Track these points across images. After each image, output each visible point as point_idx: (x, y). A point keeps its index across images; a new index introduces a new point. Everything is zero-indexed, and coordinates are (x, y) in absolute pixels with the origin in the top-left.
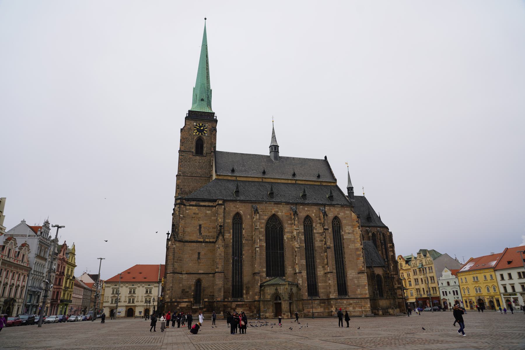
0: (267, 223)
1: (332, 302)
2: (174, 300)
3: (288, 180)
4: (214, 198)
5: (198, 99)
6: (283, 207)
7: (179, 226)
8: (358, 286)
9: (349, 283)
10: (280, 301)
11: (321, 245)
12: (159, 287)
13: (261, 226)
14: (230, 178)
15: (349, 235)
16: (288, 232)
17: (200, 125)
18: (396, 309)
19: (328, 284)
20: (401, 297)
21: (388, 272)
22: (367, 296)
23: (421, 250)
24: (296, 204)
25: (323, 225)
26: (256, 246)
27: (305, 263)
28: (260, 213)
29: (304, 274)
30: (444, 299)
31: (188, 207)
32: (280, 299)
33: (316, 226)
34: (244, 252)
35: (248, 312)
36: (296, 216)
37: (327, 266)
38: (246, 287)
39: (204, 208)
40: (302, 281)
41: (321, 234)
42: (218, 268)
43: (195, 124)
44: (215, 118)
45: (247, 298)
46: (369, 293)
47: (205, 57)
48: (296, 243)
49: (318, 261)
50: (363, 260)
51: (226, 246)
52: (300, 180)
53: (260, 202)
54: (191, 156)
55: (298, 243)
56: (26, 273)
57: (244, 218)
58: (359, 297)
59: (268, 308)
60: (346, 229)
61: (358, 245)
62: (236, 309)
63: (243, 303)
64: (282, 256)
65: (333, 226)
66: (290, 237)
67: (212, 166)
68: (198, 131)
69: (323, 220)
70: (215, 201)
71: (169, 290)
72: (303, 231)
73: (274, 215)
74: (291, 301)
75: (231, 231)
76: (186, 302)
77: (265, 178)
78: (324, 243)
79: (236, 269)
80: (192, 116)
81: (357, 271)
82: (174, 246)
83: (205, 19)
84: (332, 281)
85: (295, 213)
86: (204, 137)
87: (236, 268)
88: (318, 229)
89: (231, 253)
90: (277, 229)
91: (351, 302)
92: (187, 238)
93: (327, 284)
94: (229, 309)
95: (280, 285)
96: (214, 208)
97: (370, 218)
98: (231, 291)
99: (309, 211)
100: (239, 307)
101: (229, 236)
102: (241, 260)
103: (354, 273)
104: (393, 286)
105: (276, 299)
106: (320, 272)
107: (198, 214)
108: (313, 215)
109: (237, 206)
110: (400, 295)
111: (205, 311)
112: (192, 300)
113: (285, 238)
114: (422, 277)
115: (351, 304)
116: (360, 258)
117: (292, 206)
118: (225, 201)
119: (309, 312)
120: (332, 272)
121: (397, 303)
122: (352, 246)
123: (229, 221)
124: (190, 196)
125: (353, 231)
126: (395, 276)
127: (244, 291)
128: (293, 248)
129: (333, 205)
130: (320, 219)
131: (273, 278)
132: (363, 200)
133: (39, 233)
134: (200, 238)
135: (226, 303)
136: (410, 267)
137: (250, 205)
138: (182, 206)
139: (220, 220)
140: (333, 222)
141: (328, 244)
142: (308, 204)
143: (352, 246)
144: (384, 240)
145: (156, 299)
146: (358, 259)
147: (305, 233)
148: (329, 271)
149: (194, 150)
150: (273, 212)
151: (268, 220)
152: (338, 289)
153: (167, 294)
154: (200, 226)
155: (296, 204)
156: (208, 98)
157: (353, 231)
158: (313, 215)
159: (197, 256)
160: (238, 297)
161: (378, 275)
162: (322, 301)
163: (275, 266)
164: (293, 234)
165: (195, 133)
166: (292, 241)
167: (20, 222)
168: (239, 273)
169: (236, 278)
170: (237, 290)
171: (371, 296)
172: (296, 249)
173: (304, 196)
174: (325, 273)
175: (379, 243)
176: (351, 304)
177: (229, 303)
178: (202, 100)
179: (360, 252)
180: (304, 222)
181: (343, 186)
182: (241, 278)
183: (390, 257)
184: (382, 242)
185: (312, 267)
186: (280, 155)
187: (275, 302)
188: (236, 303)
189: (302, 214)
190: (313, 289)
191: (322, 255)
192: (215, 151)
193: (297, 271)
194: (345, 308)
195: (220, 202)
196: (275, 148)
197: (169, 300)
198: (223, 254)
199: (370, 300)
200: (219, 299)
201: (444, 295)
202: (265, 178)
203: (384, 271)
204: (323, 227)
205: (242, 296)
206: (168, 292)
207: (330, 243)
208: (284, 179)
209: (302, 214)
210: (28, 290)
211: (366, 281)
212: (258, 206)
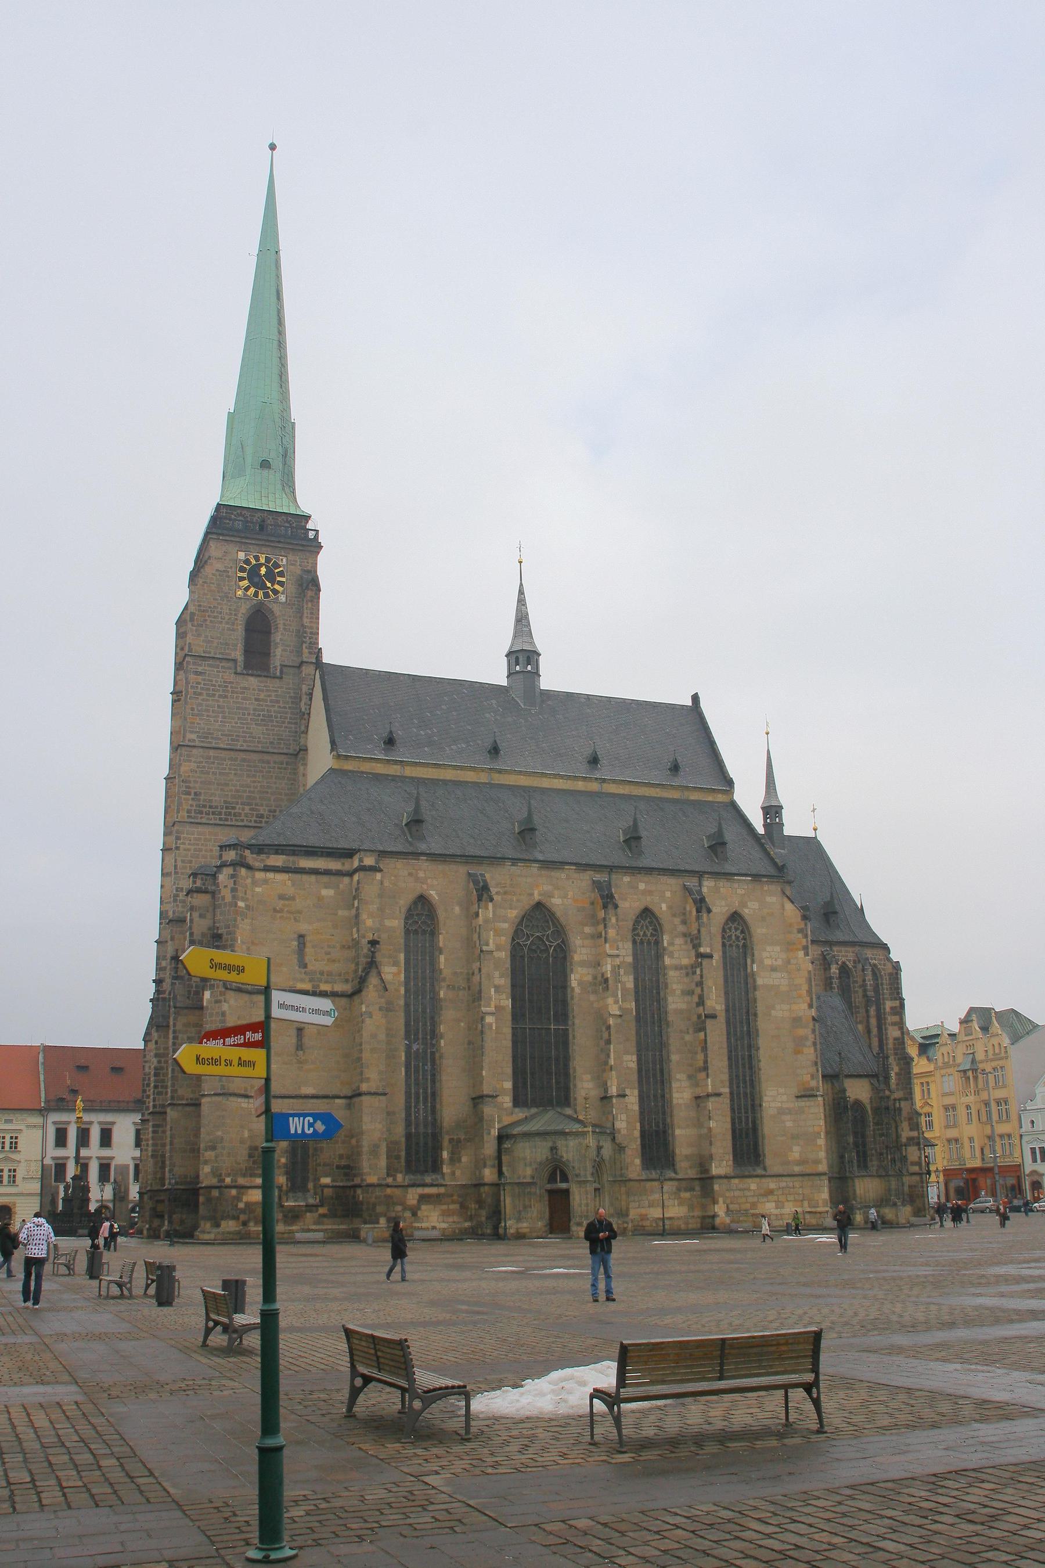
0: (517, 933)
1: (716, 1187)
2: (228, 1180)
3: (576, 778)
4: (343, 844)
5: (249, 460)
6: (568, 878)
7: (235, 940)
8: (795, 1137)
9: (769, 1128)
10: (564, 1186)
11: (684, 1006)
12: (44, 1127)
13: (497, 943)
14: (380, 769)
15: (774, 975)
16: (583, 964)
17: (258, 559)
18: (903, 1205)
19: (705, 1131)
20: (916, 1169)
21: (887, 1093)
22: (823, 1167)
23: (972, 1009)
24: (611, 869)
25: (695, 941)
26: (483, 1009)
27: (634, 1065)
28: (495, 897)
29: (633, 1099)
30: (1034, 1172)
31: (260, 875)
32: (565, 1178)
33: (671, 944)
34: (442, 1028)
35: (456, 1218)
36: (611, 911)
37: (703, 1075)
38: (451, 1140)
39: (313, 878)
40: (626, 1120)
41: (690, 970)
42: (368, 1080)
43: (242, 555)
44: (311, 535)
45: (455, 1173)
46: (827, 1158)
47: (274, 299)
48: (610, 1001)
49: (674, 1057)
50: (812, 1057)
51: (388, 1009)
52: (614, 781)
53: (496, 860)
54: (229, 676)
55: (616, 1002)
57: (441, 914)
58: (797, 1169)
59: (525, 1207)
60: (765, 954)
61: (803, 1009)
62: (419, 1209)
63: (442, 1190)
64: (564, 1040)
65: (724, 945)
66: (589, 978)
67: (305, 716)
68: (253, 583)
69: (695, 926)
70: (349, 854)
71: (213, 1148)
72: (630, 959)
73: (539, 905)
74: (597, 1185)
75: (402, 956)
77: (500, 771)
78: (696, 999)
79: (417, 1084)
80: (226, 524)
81: (794, 1091)
82: (225, 1007)
83: (273, 147)
84: (720, 1124)
85: (608, 900)
86: (276, 609)
87: (417, 1079)
88: (676, 954)
89: (402, 1032)
90: (547, 950)
93: (701, 1127)
95: (563, 1134)
96: (346, 880)
97: (836, 913)
98: (403, 1154)
99: (650, 893)
100: (428, 1203)
101: (393, 972)
102: (433, 1054)
103: (784, 1098)
104: (898, 1136)
105: (552, 1179)
106: (681, 1094)
107: (293, 898)
108: (664, 906)
109: (421, 874)
110: (913, 1164)
111: (324, 1216)
113: (574, 984)
114: (971, 1099)
115: (771, 1192)
116: (806, 1050)
117: (598, 877)
118: (383, 854)
119: (644, 1217)
120: (719, 1095)
121: (906, 1189)
122: (781, 1011)
123: (396, 923)
124: (265, 837)
126: (903, 1103)
127: (445, 1154)
128: (600, 1018)
129: (728, 876)
130: (684, 922)
131: (534, 1110)
132: (811, 849)
134: (302, 980)
135: (389, 1191)
136: (931, 1068)
137: (462, 870)
138: (243, 871)
139: (369, 923)
140: (724, 931)
141: (709, 1003)
142: (649, 871)
143: (781, 1011)
144: (876, 988)
145: (36, 1170)
146: (797, 1052)
147: (637, 967)
148: (710, 1089)
149: (238, 655)
150: (537, 897)
151: (520, 923)
153: (206, 1162)
155: (611, 869)
156: (285, 456)
158: (664, 906)
159: (294, 1040)
160: (426, 1171)
161: (858, 1103)
162: (684, 1184)
163: (543, 1072)
164: (599, 968)
165: (242, 590)
166: (595, 992)
168: (425, 1092)
169: (418, 1112)
170: (421, 1152)
171: (830, 1166)
172: (611, 1021)
173: (633, 839)
174: (697, 1098)
175: (858, 999)
176: (771, 1192)
177: (397, 1192)
178: (265, 464)
179: (806, 1031)
180: (634, 929)
181: (749, 800)
182: (433, 1108)
183: (891, 1041)
184: (870, 994)
185: (654, 1075)
186: (547, 682)
187: (549, 1186)
188: (420, 1190)
191: (687, 1038)
192: (319, 664)
193: (613, 1090)
194: (754, 1205)
195: (369, 861)
196: (524, 659)
197: (214, 1181)
198: (382, 1036)
199: (830, 1179)
200: (372, 1179)
201: (1034, 1160)
202: (500, 771)
203: (875, 1089)
204: (696, 947)
205: (436, 1166)
206: (209, 1155)
207: (715, 1002)
208: (562, 777)
209: (629, 904)
211: (822, 1123)
212: (487, 876)
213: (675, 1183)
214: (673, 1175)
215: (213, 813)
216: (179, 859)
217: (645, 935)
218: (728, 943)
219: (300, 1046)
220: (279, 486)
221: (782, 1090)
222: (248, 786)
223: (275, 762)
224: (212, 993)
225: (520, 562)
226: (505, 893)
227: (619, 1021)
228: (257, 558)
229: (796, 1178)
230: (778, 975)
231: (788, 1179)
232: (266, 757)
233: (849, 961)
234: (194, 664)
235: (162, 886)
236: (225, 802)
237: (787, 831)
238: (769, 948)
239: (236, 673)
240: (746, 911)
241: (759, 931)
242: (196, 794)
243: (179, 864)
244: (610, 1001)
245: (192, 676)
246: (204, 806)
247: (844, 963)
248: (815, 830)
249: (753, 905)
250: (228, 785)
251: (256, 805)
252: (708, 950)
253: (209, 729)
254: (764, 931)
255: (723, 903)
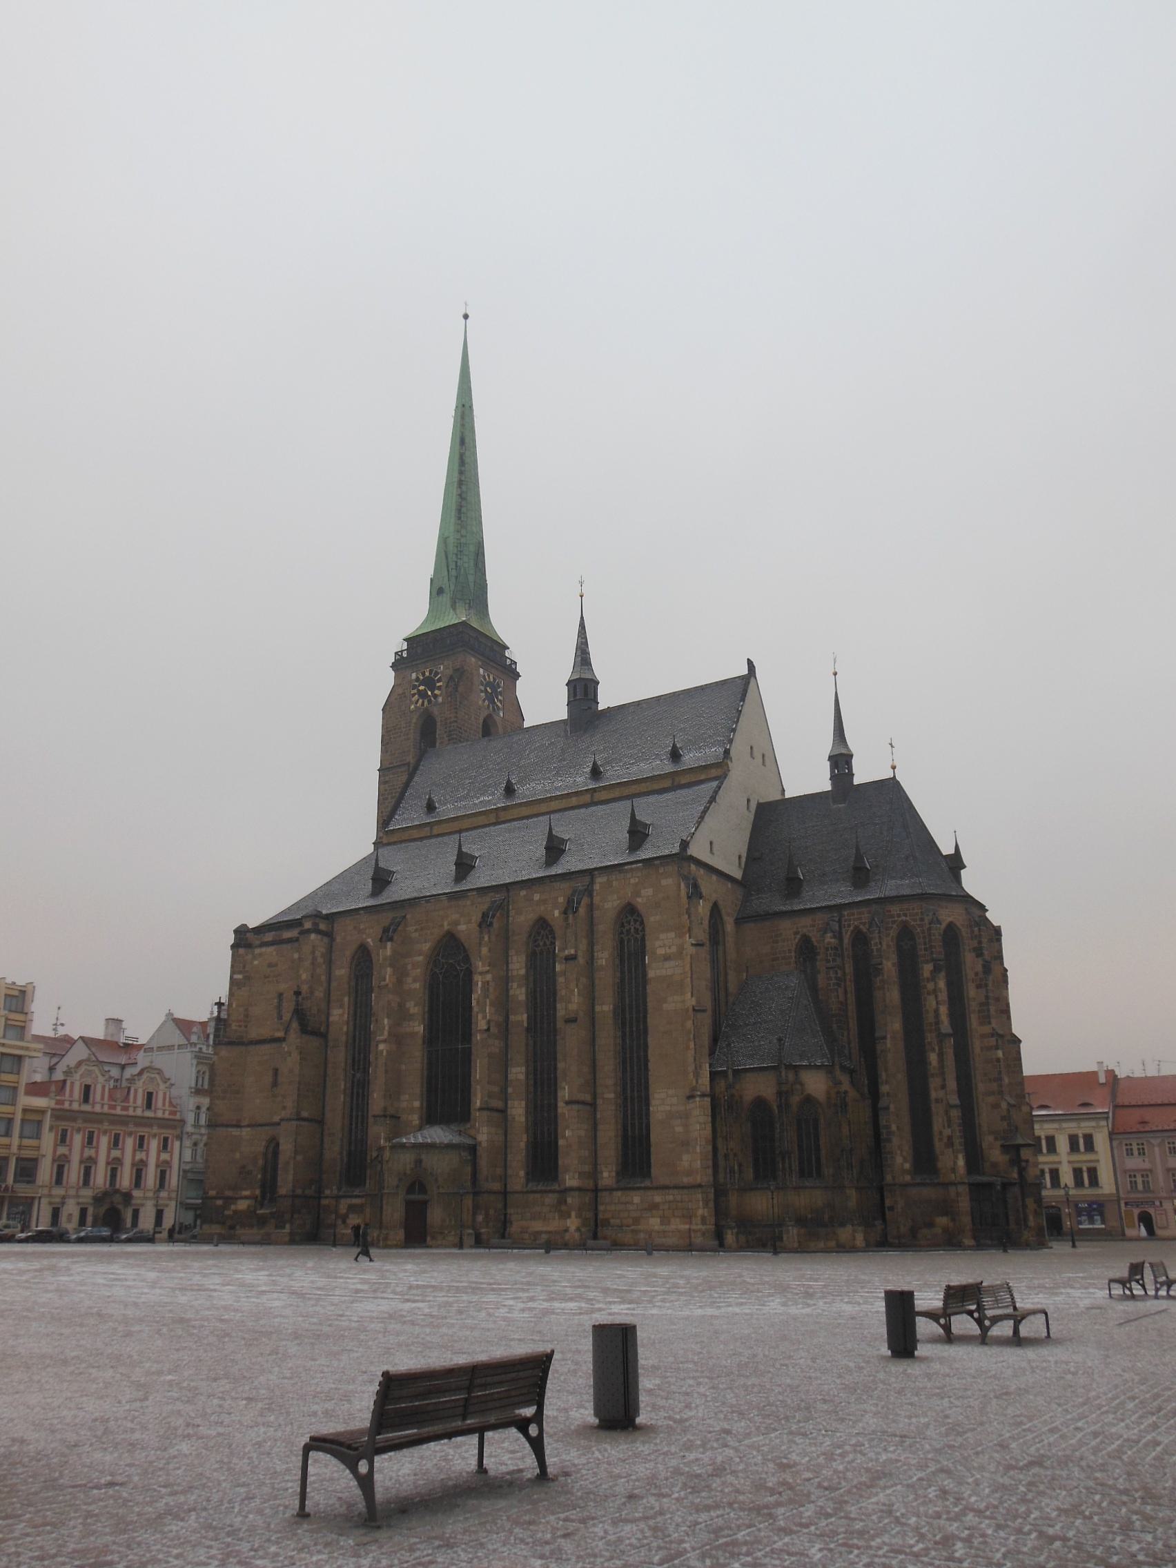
2: (212, 1193)
15: (667, 964)
27: (522, 1077)
31: (257, 951)
39: (289, 946)
42: (284, 1108)
43: (414, 676)
55: (485, 1017)
56: (167, 1133)
60: (658, 943)
65: (622, 941)
72: (523, 972)
75: (346, 999)
76: (246, 1197)
80: (419, 653)
83: (466, 317)
86: (435, 711)
91: (658, 1199)
92: (254, 1034)
94: (333, 1216)
99: (544, 902)
103: (675, 1100)
107: (276, 965)
109: (362, 927)
112: (258, 1192)
115: (654, 1207)
123: (342, 972)
125: (681, 948)
133: (194, 1039)
134: (278, 1030)
138: (241, 951)
139: (304, 976)
150: (446, 927)
152: (556, 1158)
154: (280, 995)
157: (681, 948)
158: (556, 913)
161: (760, 1103)
167: (163, 1018)
176: (654, 1207)
179: (689, 1024)
188: (349, 1201)
189: (522, 918)
190: (544, 1161)
194: (636, 1221)
196: (582, 689)
203: (780, 1084)
210: (185, 1171)
213: (556, 1195)
214: (556, 1187)
217: (545, 944)
218: (626, 938)
219: (275, 1084)
220: (449, 605)
221: (671, 1092)
226: (422, 929)
227: (485, 1035)
228: (423, 674)
229: (685, 1191)
230: (672, 963)
231: (676, 1191)
233: (864, 924)
237: (856, 781)
238: (662, 936)
240: (639, 900)
241: (652, 919)
244: (480, 1017)
247: (856, 927)
248: (894, 768)
249: (648, 892)
252: (572, 952)
254: (658, 918)
255: (615, 897)
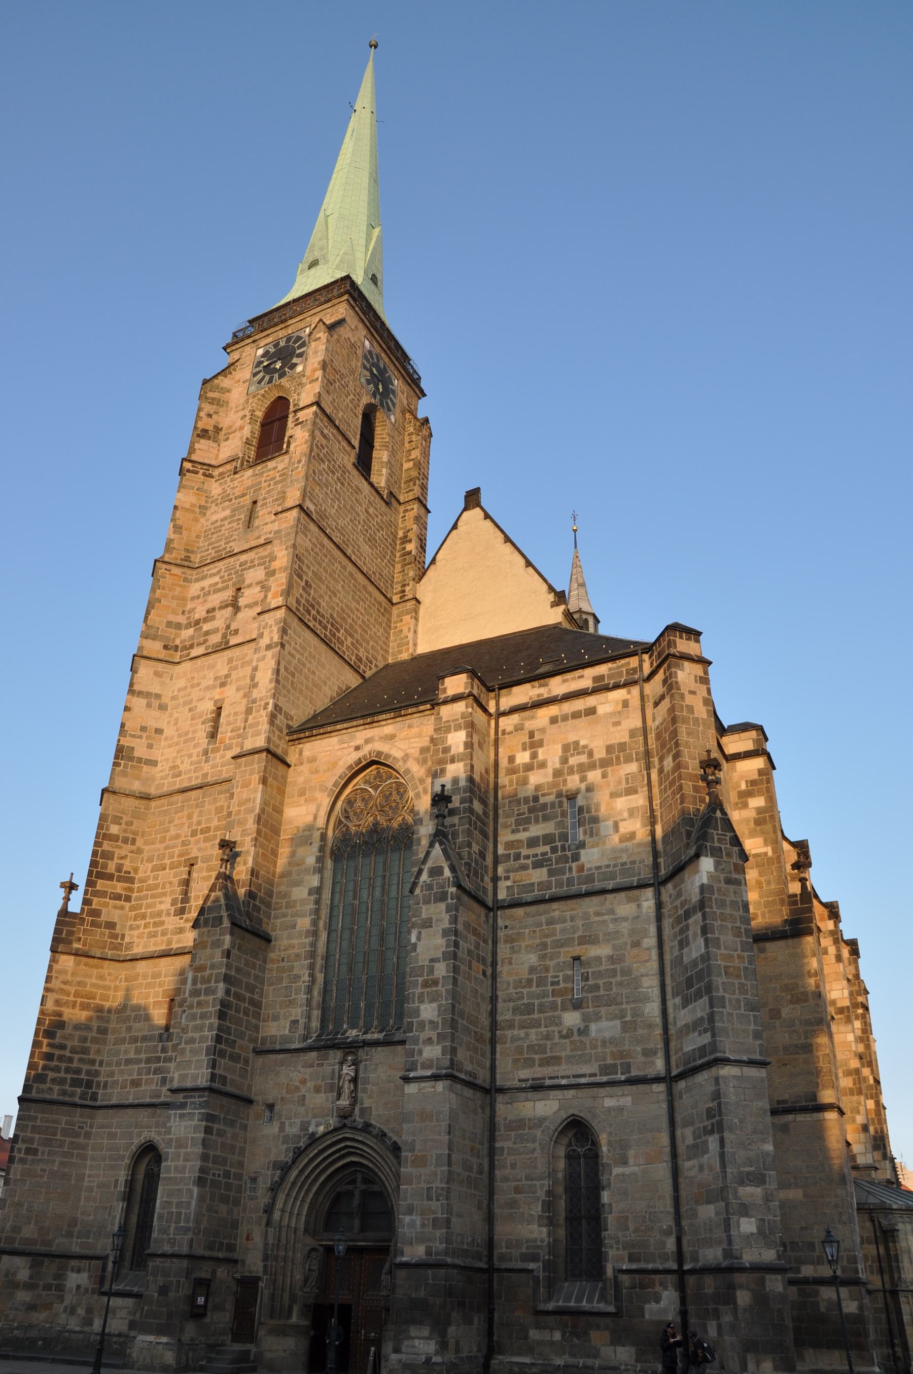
215: (320, 623)
216: (283, 664)
222: (351, 610)
223: (375, 599)
224: (717, 865)
225: (575, 531)
232: (371, 588)
234: (322, 421)
235: (127, 709)
236: (331, 615)
239: (354, 464)
242: (307, 582)
243: (282, 670)
245: (317, 433)
246: (313, 607)
250: (335, 595)
251: (357, 641)
253: (325, 510)
